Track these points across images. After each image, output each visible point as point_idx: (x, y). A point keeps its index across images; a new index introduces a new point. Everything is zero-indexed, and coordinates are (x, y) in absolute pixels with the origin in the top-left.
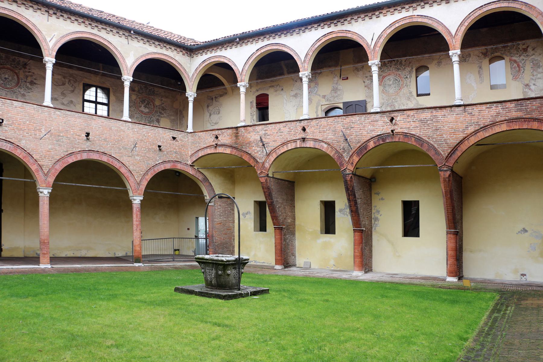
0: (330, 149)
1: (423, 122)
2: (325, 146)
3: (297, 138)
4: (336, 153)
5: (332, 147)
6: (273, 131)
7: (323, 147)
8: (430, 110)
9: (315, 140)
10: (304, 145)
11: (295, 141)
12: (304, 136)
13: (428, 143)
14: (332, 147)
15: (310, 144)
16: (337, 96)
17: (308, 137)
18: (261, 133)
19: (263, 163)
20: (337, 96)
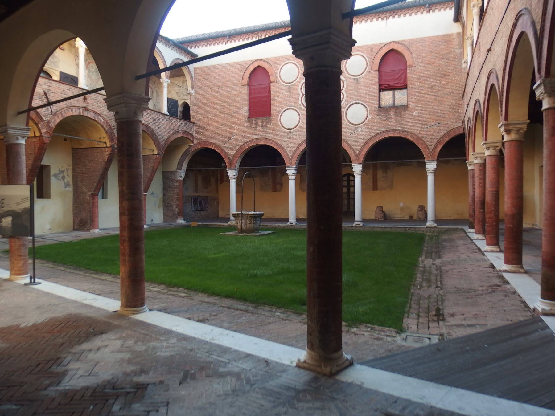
0: (106, 124)
1: (154, 120)
2: (103, 120)
3: (80, 105)
4: (109, 129)
5: (107, 123)
6: (58, 90)
7: (101, 121)
8: (157, 114)
9: (95, 113)
10: (86, 114)
11: (79, 108)
12: (85, 105)
13: (156, 135)
14: (107, 123)
15: (90, 115)
16: (53, 63)
17: (89, 108)
18: (44, 86)
19: (48, 122)
20: (53, 63)
